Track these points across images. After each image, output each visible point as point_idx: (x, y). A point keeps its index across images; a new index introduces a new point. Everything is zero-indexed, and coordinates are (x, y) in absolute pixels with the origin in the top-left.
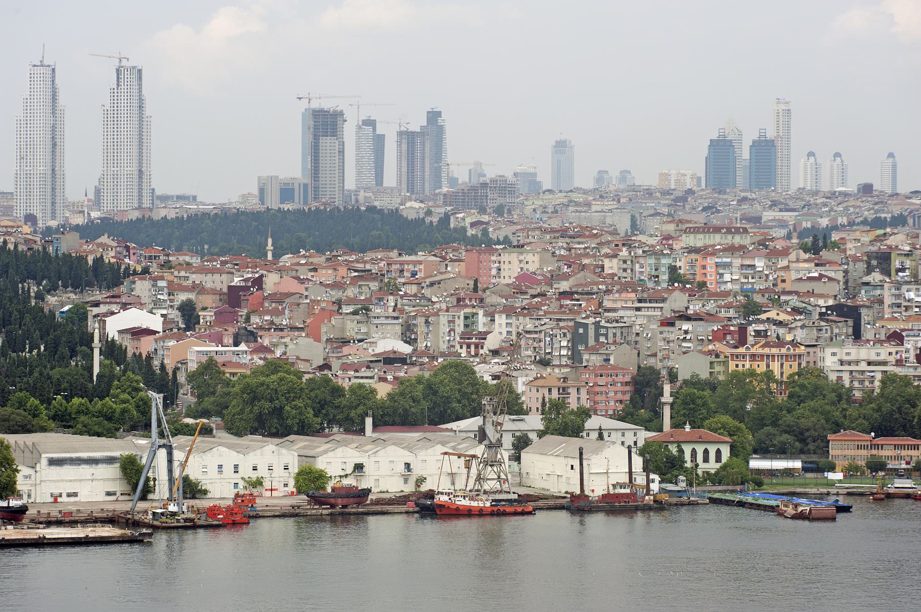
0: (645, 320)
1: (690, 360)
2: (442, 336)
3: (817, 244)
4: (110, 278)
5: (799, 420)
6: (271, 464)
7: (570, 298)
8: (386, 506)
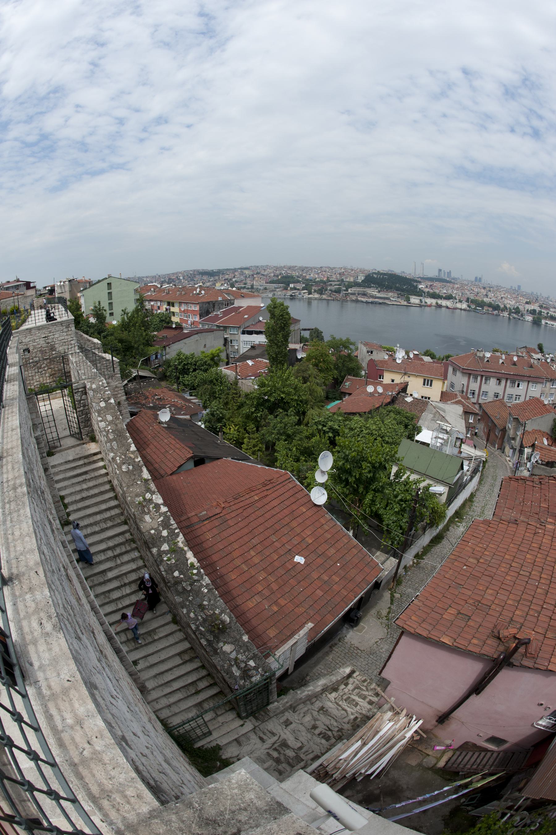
0: (468, 293)
1: (472, 297)
5: (482, 304)
6: (433, 301)
8: (444, 307)
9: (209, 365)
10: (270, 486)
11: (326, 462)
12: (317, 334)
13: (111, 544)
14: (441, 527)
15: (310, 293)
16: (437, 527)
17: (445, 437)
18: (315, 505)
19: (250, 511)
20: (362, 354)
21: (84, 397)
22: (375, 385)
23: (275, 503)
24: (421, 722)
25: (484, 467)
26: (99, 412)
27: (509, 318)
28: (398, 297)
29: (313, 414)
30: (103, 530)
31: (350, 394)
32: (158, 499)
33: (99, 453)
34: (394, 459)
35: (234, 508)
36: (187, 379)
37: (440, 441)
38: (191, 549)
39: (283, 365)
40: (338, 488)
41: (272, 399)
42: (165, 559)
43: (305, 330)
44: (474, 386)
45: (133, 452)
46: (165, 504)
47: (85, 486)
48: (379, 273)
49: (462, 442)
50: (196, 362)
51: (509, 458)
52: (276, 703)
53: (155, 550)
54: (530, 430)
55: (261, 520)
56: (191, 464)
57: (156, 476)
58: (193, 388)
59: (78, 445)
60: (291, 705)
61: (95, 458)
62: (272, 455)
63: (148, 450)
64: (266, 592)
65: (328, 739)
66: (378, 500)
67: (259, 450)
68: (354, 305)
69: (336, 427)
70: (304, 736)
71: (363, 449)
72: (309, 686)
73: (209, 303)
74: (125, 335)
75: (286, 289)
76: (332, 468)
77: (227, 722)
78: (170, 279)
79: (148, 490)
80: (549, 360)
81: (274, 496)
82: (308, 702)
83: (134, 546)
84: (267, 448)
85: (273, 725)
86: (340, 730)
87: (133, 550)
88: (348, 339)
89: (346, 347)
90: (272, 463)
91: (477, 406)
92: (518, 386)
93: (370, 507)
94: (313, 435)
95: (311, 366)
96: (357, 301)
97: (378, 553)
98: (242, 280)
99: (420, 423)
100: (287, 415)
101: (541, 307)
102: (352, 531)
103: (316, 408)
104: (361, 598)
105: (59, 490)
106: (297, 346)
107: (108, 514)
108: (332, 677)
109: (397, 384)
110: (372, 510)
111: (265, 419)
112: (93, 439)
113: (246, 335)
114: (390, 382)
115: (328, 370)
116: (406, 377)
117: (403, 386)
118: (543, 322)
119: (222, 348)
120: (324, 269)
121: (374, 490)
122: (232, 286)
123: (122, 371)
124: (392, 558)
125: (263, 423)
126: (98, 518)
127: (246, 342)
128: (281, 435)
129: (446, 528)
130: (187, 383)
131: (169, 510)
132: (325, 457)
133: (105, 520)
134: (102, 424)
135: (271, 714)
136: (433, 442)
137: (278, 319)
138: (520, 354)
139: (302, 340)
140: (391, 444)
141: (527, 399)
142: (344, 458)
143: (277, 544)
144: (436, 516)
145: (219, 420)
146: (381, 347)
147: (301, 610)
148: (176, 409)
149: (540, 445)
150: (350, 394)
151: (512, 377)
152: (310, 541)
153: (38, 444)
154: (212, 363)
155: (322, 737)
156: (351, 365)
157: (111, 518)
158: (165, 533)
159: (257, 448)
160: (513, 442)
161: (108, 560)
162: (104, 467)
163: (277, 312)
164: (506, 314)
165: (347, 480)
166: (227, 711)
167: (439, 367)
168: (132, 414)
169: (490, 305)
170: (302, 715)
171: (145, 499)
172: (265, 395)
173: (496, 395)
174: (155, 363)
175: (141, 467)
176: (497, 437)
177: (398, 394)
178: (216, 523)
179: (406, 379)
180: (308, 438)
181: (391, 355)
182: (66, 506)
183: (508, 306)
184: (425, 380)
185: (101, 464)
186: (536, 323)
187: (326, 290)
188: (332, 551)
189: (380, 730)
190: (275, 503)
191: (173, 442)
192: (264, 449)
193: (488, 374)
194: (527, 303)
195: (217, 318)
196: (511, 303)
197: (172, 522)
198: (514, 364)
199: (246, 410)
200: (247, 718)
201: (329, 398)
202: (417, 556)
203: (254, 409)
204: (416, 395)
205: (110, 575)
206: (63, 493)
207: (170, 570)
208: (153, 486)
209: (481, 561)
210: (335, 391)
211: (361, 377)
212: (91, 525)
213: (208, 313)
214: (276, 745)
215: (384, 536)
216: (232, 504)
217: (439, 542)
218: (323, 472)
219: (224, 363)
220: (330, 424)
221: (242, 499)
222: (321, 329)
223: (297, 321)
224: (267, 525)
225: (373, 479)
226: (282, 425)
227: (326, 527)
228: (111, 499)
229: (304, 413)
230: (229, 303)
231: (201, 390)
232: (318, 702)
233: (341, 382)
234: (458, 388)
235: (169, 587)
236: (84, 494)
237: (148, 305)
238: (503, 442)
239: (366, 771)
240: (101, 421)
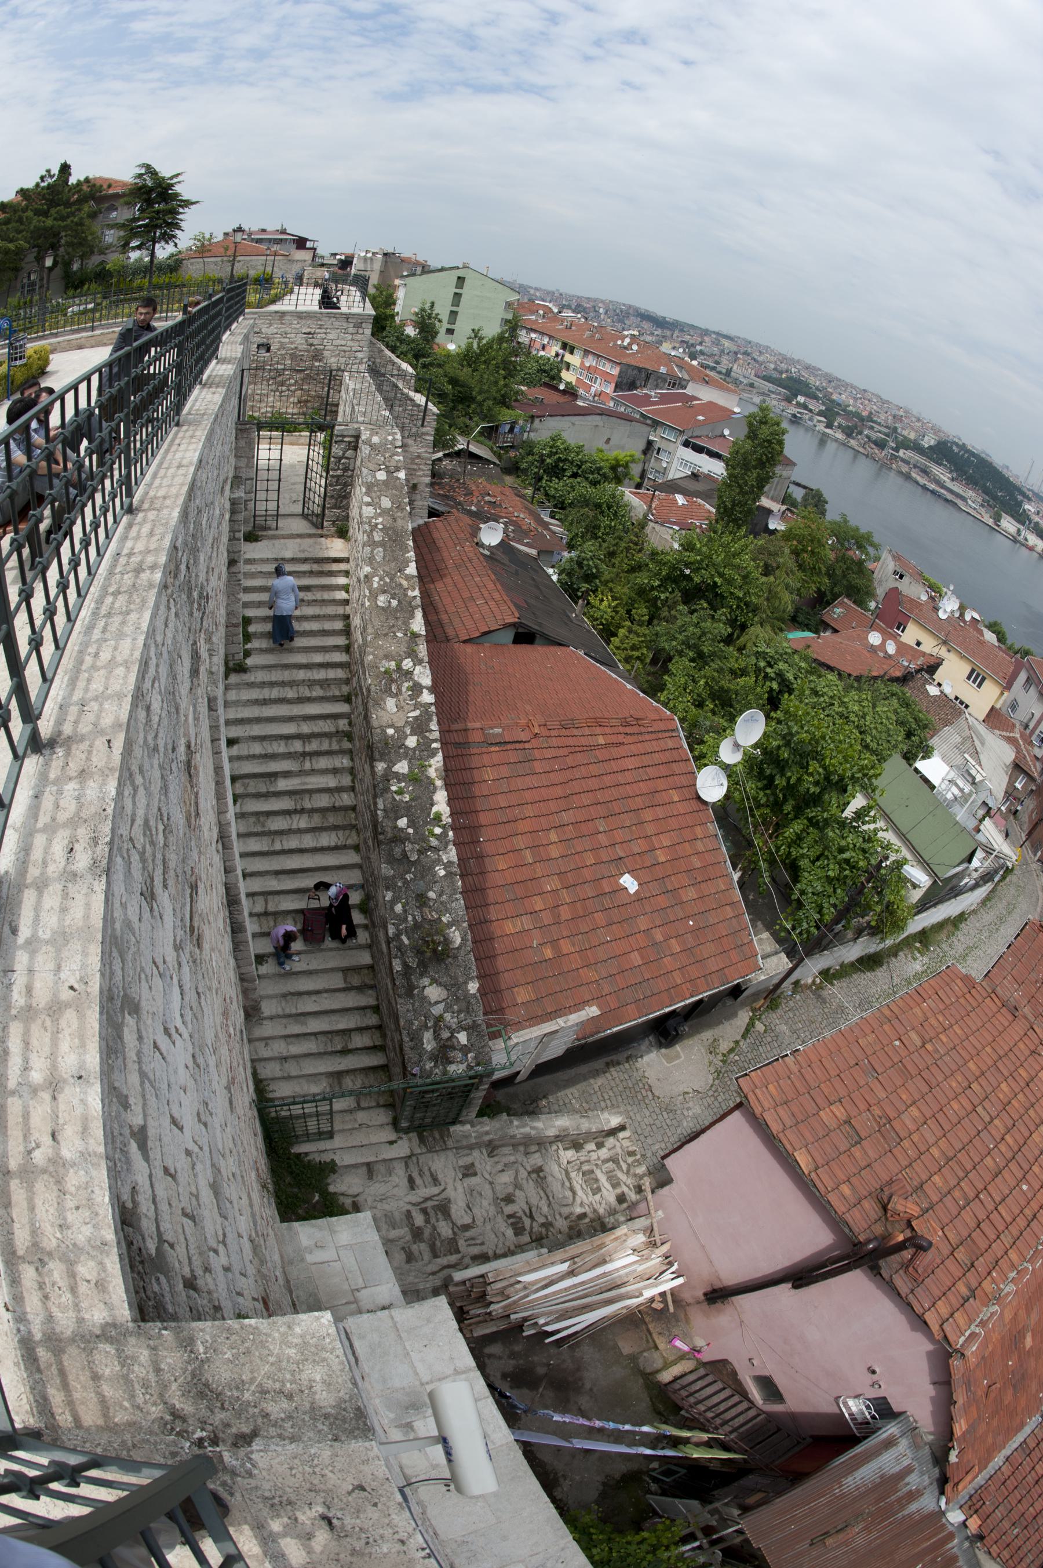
9: (604, 476)
11: (750, 729)
12: (816, 500)
13: (306, 728)
15: (829, 426)
18: (699, 798)
19: (580, 758)
20: (883, 571)
21: (350, 453)
22: (886, 636)
23: (630, 763)
24: (680, 1281)
26: (369, 487)
28: (982, 506)
29: (759, 635)
30: (300, 700)
31: (835, 631)
32: (424, 676)
33: (346, 560)
34: (866, 782)
35: (554, 742)
36: (556, 486)
37: (956, 791)
38: (448, 786)
40: (751, 786)
41: (697, 580)
45: (408, 578)
46: (433, 690)
48: (963, 447)
50: (582, 462)
52: (468, 1127)
55: (593, 784)
56: (510, 635)
57: (436, 634)
58: (561, 505)
59: (310, 536)
60: (490, 1142)
61: (335, 567)
63: (439, 585)
64: (546, 918)
65: (518, 1231)
67: (638, 658)
68: (900, 480)
69: (790, 676)
70: (484, 1207)
71: (823, 738)
72: (539, 1120)
76: (756, 746)
77: (368, 1126)
79: (412, 654)
82: (522, 1148)
83: (346, 745)
85: (444, 1165)
86: (547, 1225)
87: (342, 752)
89: (860, 547)
93: (789, 847)
94: (743, 672)
95: (787, 551)
96: (907, 477)
97: (766, 935)
100: (713, 617)
103: (768, 628)
105: (246, 605)
106: (775, 507)
107: (321, 675)
108: (583, 1120)
109: (924, 654)
110: (789, 853)
111: (670, 608)
112: (342, 533)
113: (689, 450)
114: (913, 644)
116: (944, 649)
117: (932, 661)
121: (810, 820)
123: (439, 433)
125: (665, 613)
127: (685, 463)
128: (689, 647)
130: (552, 492)
131: (435, 704)
132: (752, 719)
133: (311, 683)
135: (450, 1143)
140: (873, 752)
142: (784, 737)
143: (603, 839)
145: (588, 578)
146: (921, 574)
147: (591, 975)
150: (835, 631)
152: (662, 859)
153: (233, 512)
154: (611, 475)
155: (512, 1224)
156: (859, 582)
157: (324, 683)
158: (412, 742)
159: (636, 654)
161: (289, 756)
162: (346, 588)
165: (771, 779)
166: (378, 1106)
167: (1008, 662)
168: (433, 513)
170: (500, 1167)
171: (399, 668)
172: (687, 565)
175: (414, 608)
177: (918, 671)
178: (512, 757)
179: (943, 652)
180: (735, 674)
181: (932, 598)
184: (973, 671)
185: (342, 581)
187: (860, 433)
188: (691, 893)
189: (611, 1261)
190: (630, 763)
191: (491, 586)
192: (648, 661)
195: (646, 400)
197: (434, 726)
199: (642, 579)
200: (406, 1133)
201: (796, 621)
203: (657, 583)
204: (947, 689)
205: (282, 785)
206: (250, 613)
207: (395, 810)
208: (422, 650)
209: (929, 1046)
210: (811, 614)
211: (867, 609)
212: (283, 684)
214: (429, 1204)
215: (789, 910)
216: (554, 733)
218: (737, 745)
219: (633, 483)
220: (782, 666)
221: (576, 732)
222: (827, 495)
224: (600, 796)
225: (816, 800)
226: (697, 631)
227: (700, 846)
228: (336, 648)
229: (743, 627)
231: (573, 514)
232: (537, 1155)
233: (828, 604)
235: (379, 843)
239: (547, 1324)
240: (368, 504)
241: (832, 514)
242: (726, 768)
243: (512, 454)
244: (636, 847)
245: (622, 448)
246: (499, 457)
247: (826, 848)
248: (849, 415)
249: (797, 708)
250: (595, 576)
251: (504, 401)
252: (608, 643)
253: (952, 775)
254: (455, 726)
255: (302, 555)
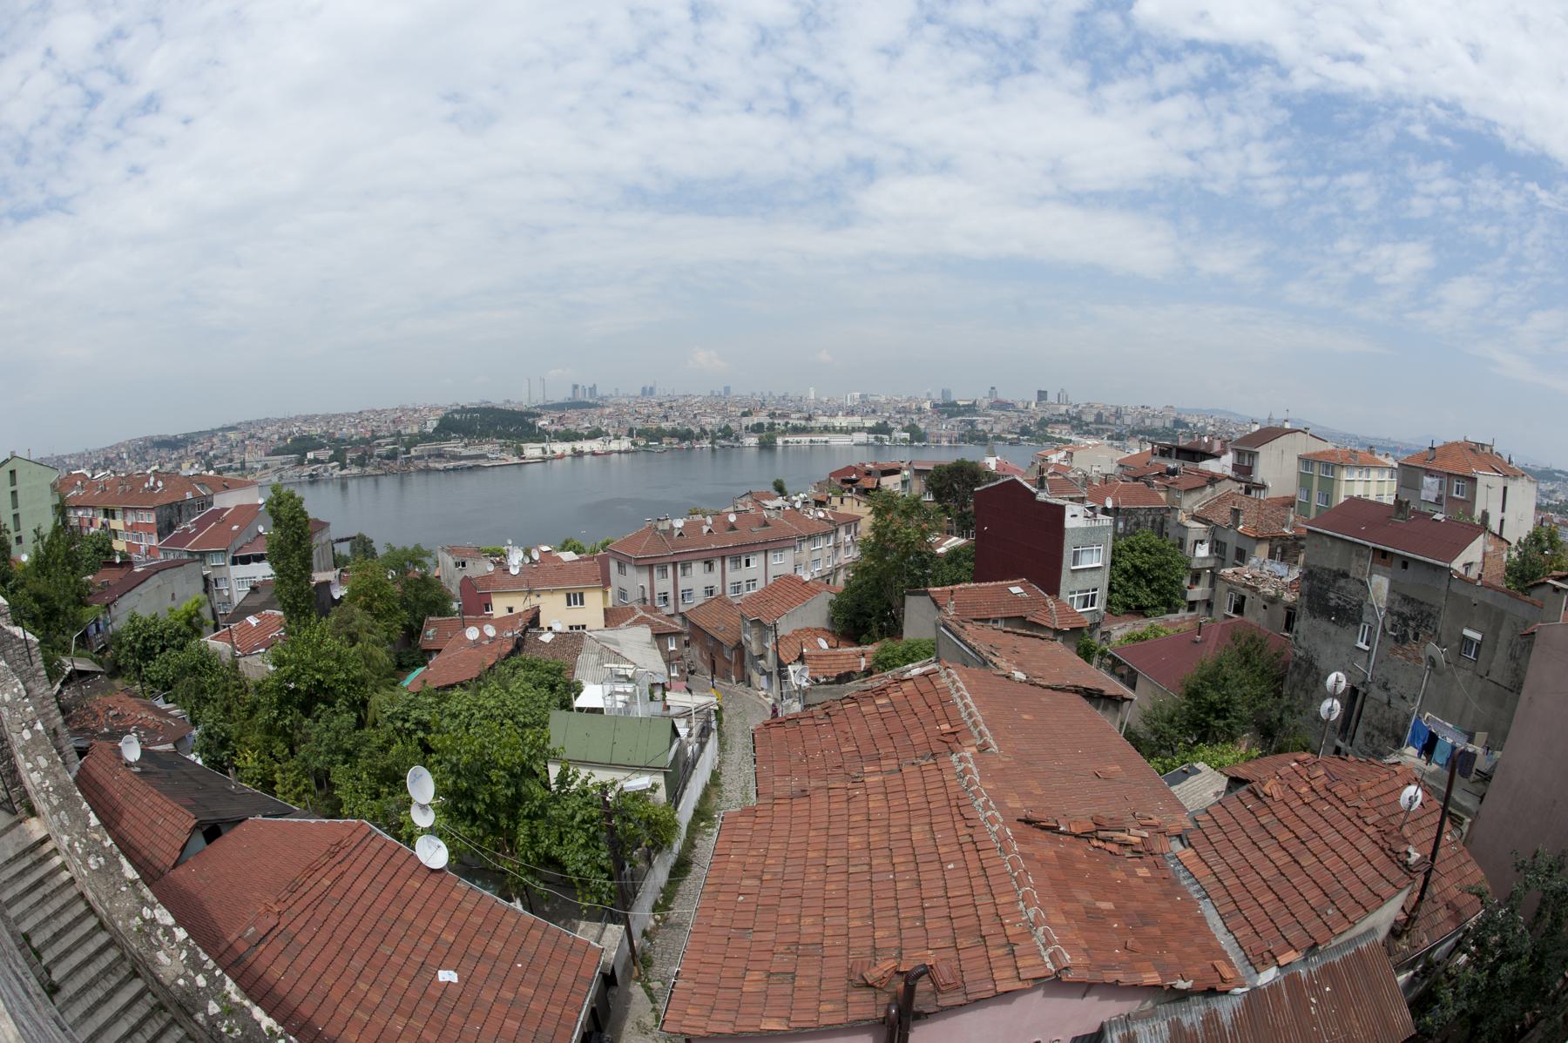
0: (630, 419)
1: (638, 425)
2: (596, 423)
3: (660, 405)
4: (539, 415)
5: (658, 435)
7: (618, 416)
9: (185, 635)
10: (343, 854)
11: (422, 786)
12: (362, 545)
14: (677, 846)
15: (343, 467)
16: (670, 847)
17: (629, 688)
18: (433, 871)
19: (324, 909)
20: (446, 570)
22: (479, 624)
23: (361, 884)
25: (720, 720)
26: (24, 750)
27: (713, 450)
29: (380, 701)
30: (110, 994)
31: (439, 651)
35: (296, 909)
36: (154, 668)
37: (620, 697)
39: (309, 616)
40: (462, 828)
41: (303, 688)
42: (224, 1030)
43: (341, 540)
44: (664, 584)
45: (96, 829)
47: (49, 910)
48: (464, 410)
49: (664, 688)
50: (163, 631)
51: (764, 693)
53: (200, 1017)
54: (788, 633)
55: (350, 922)
56: (199, 840)
57: (150, 874)
58: (167, 686)
59: (14, 825)
62: (329, 795)
63: (124, 824)
66: (541, 831)
68: (422, 478)
69: (427, 717)
71: (483, 747)
73: (170, 505)
74: (41, 585)
75: (300, 463)
76: (436, 796)
78: (106, 459)
79: (144, 902)
80: (798, 505)
81: (354, 871)
83: (168, 1016)
84: (319, 785)
88: (417, 547)
89: (417, 563)
90: (335, 811)
91: (678, 620)
92: (748, 563)
94: (390, 742)
95: (358, 610)
96: (428, 471)
97: (582, 925)
98: (220, 455)
99: (578, 675)
100: (335, 713)
101: (772, 415)
102: (518, 901)
103: (383, 690)
104: (593, 1012)
105: (18, 921)
106: (330, 576)
109: (519, 615)
111: (299, 728)
112: (32, 812)
113: (239, 566)
114: (506, 613)
115: (391, 611)
118: (780, 441)
119: (202, 596)
120: (365, 416)
121: (528, 817)
122: (209, 467)
123: (48, 662)
124: (610, 926)
126: (92, 970)
127: (241, 580)
128: (335, 753)
129: (690, 844)
130: (154, 677)
131: (191, 935)
132: (417, 777)
134: (36, 777)
136: (609, 703)
137: (288, 527)
138: (741, 508)
139: (338, 562)
140: (532, 726)
141: (770, 581)
142: (451, 772)
143: (397, 959)
144: (659, 831)
145: (223, 744)
146: (479, 550)
148: (148, 735)
149: (814, 652)
150: (439, 651)
151: (732, 551)
152: (451, 939)
154: (189, 631)
159: (301, 788)
160: (762, 662)
162: (64, 867)
163: (284, 511)
164: (706, 444)
165: (471, 811)
168: (82, 753)
169: (674, 434)
172: (288, 680)
173: (710, 591)
174: (97, 641)
175: (116, 857)
176: (730, 662)
177: (524, 633)
178: (279, 944)
179: (534, 601)
180: (384, 749)
181: (500, 563)
182: (38, 953)
183: (708, 428)
184: (568, 596)
185: (57, 860)
186: (767, 446)
187: (371, 456)
188: (497, 945)
190: (361, 884)
191: (159, 801)
192: (314, 788)
193: (685, 558)
194: (744, 415)
195: (187, 536)
196: (712, 422)
197: (204, 957)
198: (733, 527)
199: (262, 717)
201: (403, 667)
202: (656, 908)
203: (276, 713)
204: (558, 628)
206: (25, 927)
210: (411, 652)
211: (453, 614)
213: (171, 527)
216: (290, 902)
217: (687, 872)
218: (423, 807)
219: (211, 628)
220: (414, 714)
222: (369, 535)
223: (322, 526)
224: (365, 927)
225: (518, 799)
226: (331, 734)
229: (364, 703)
230: (205, 502)
231: (180, 688)
233: (419, 632)
234: (634, 595)
236: (56, 926)
237: (74, 517)
238: (743, 667)
240: (33, 770)
241: (381, 551)
242: (431, 831)
243: (108, 655)
244: (425, 945)
245: (186, 597)
246: (101, 664)
247: (560, 824)
248: (355, 444)
249: (443, 741)
250: (227, 739)
251: (81, 602)
252: (274, 793)
253: (608, 688)
254: (223, 947)
255: (19, 850)
